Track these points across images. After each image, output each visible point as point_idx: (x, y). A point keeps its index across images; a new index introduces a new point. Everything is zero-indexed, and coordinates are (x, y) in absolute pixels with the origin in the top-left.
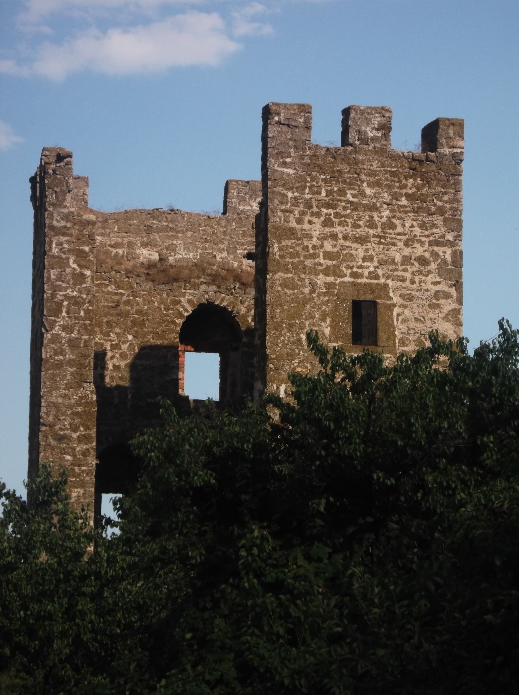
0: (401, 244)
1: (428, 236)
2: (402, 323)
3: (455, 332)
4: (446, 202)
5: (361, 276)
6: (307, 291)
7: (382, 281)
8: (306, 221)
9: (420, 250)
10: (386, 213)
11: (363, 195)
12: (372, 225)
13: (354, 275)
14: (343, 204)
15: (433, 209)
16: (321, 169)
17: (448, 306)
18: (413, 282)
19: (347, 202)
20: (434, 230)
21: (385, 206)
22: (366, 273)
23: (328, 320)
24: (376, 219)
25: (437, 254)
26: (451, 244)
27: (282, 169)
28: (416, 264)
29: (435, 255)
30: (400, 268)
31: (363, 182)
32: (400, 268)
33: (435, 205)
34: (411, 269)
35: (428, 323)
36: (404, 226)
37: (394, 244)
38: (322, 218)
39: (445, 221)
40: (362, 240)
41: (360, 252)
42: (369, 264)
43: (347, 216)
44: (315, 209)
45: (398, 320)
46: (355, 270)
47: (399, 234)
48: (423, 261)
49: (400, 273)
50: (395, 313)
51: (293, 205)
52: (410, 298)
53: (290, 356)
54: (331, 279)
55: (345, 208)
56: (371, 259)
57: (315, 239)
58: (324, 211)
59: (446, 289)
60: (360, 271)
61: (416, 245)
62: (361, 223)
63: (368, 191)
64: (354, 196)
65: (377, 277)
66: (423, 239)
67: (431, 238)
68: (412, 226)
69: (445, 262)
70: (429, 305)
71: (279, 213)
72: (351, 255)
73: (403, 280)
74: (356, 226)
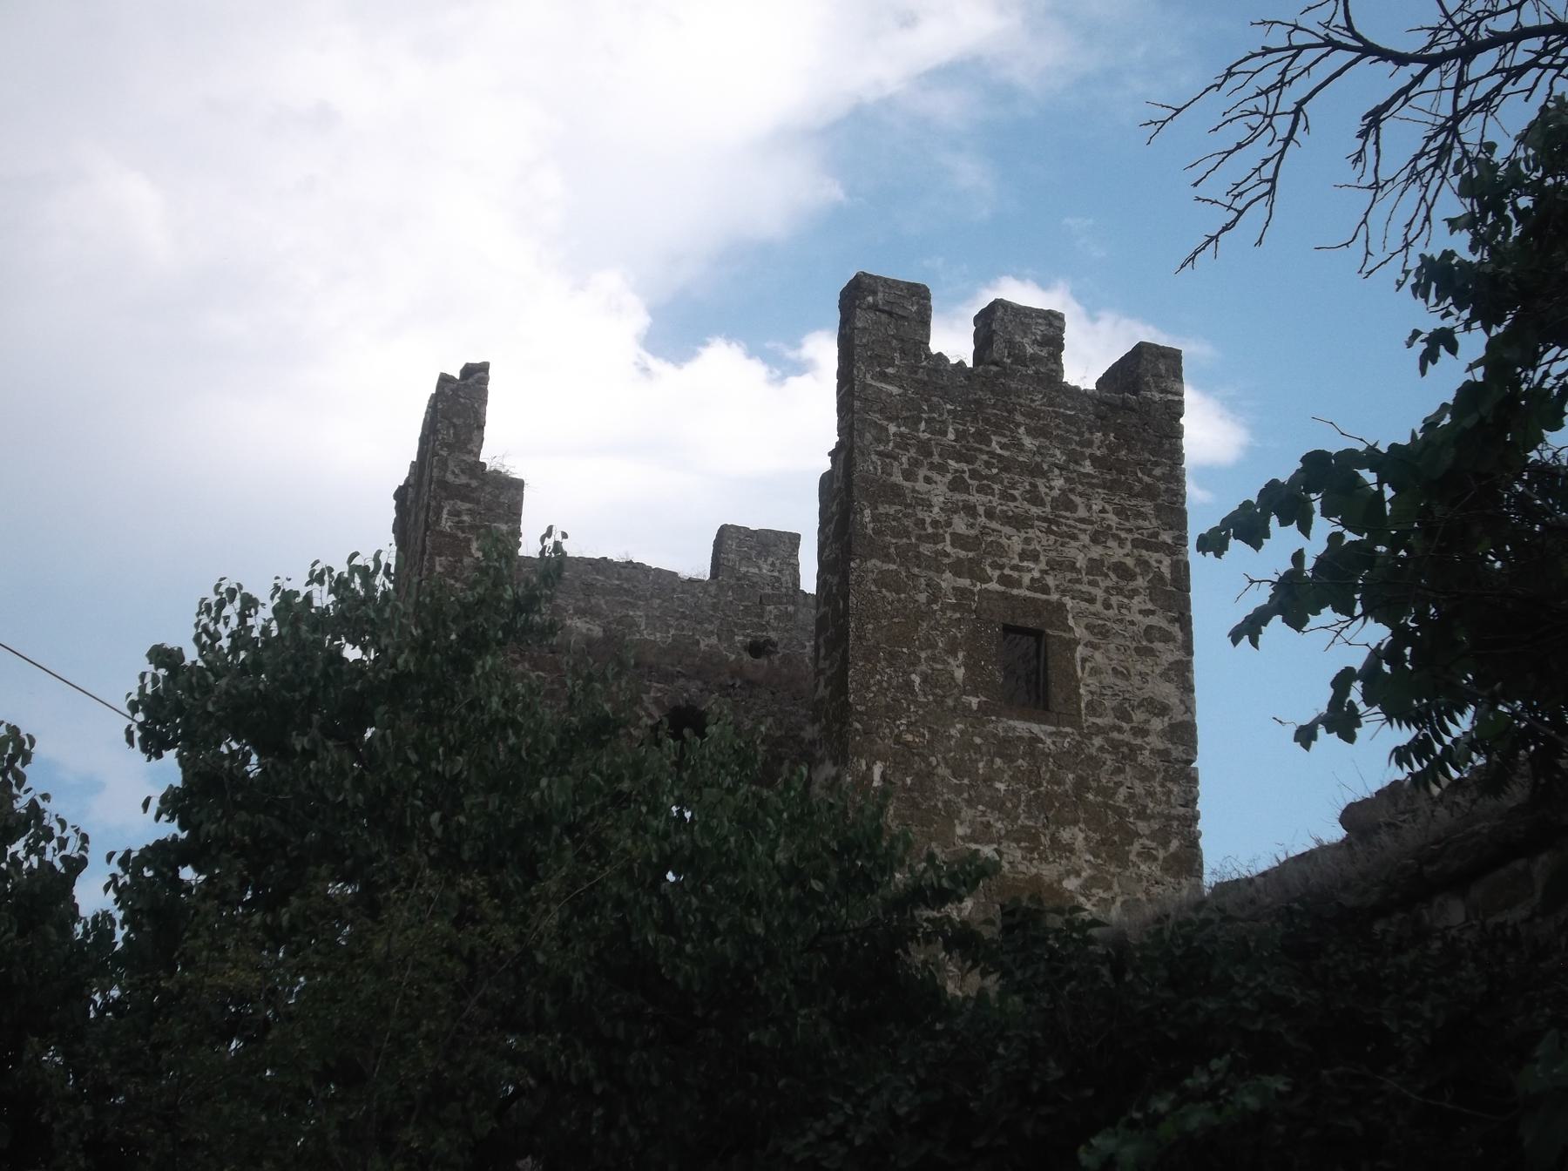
0: (1085, 538)
2: (1090, 675)
3: (1182, 701)
5: (1018, 584)
6: (922, 598)
7: (1055, 597)
8: (921, 477)
9: (1117, 553)
10: (1059, 483)
11: (1020, 447)
12: (1036, 500)
13: (1005, 580)
14: (985, 457)
18: (1108, 606)
19: (992, 454)
20: (1141, 522)
21: (1057, 472)
22: (1026, 579)
23: (961, 655)
24: (1043, 489)
29: (1143, 564)
30: (1085, 579)
31: (1018, 425)
33: (1140, 481)
36: (1089, 508)
37: (1074, 538)
38: (950, 476)
39: (1159, 509)
41: (1015, 542)
44: (936, 459)
45: (1083, 669)
46: (1007, 571)
47: (1082, 520)
48: (1121, 570)
49: (1085, 588)
50: (1078, 655)
51: (897, 446)
52: (1104, 633)
53: (893, 711)
54: (965, 582)
55: (988, 465)
56: (1035, 558)
57: (936, 510)
59: (1164, 624)
60: (1015, 574)
61: (1111, 543)
62: (1016, 493)
63: (1028, 442)
65: (1045, 590)
66: (1123, 535)
68: (1103, 511)
70: (1136, 649)
71: (874, 457)
72: (1000, 545)
73: (1092, 601)
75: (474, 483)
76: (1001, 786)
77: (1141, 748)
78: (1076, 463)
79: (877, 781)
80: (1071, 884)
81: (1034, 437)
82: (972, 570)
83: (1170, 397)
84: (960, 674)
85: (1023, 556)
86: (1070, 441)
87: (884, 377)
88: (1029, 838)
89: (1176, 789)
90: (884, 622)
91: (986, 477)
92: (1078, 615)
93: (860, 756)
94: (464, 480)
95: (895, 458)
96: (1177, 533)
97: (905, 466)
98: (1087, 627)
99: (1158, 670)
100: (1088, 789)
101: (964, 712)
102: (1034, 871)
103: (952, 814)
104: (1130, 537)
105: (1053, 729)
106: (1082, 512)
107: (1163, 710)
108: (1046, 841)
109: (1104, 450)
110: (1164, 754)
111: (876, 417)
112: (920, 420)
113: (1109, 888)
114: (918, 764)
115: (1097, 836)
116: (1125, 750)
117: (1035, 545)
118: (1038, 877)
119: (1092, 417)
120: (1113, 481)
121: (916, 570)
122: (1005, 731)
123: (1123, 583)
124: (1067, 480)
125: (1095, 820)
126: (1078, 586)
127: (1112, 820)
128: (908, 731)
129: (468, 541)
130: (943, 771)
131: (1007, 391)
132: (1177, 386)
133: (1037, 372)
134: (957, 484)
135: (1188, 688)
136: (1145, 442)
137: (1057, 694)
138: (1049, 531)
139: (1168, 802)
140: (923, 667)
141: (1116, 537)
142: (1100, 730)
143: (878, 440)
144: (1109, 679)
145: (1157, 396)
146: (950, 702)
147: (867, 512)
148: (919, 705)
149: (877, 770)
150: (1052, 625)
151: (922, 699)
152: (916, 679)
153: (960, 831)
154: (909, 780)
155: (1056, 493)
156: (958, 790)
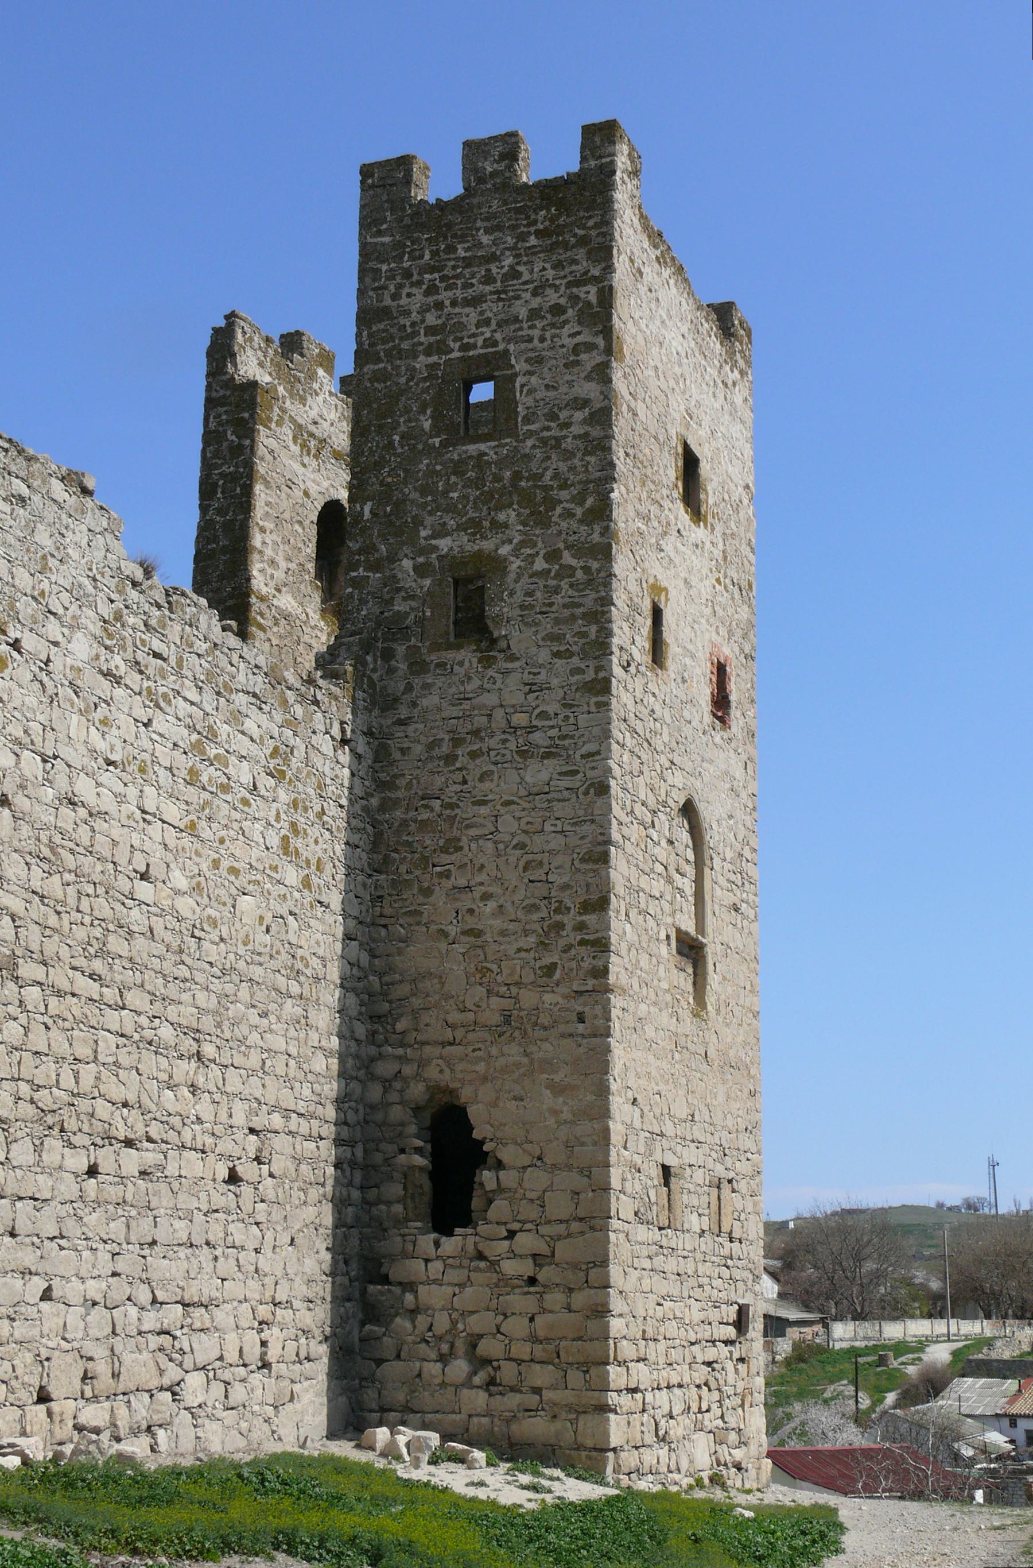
0: (527, 296)
1: (565, 277)
2: (527, 394)
3: (602, 393)
4: (592, 228)
5: (474, 346)
6: (403, 380)
7: (501, 347)
8: (404, 295)
9: (552, 297)
10: (508, 261)
11: (480, 245)
12: (488, 279)
13: (465, 348)
14: (453, 263)
15: (573, 240)
16: (423, 227)
17: (590, 360)
18: (542, 339)
19: (457, 259)
20: (574, 268)
21: (508, 253)
22: (480, 343)
23: (428, 412)
24: (494, 270)
25: (578, 297)
26: (596, 280)
27: (375, 240)
28: (549, 316)
29: (574, 299)
30: (525, 325)
31: (478, 230)
32: (525, 325)
34: (539, 324)
35: (563, 389)
36: (532, 272)
37: (518, 298)
38: (424, 287)
39: (589, 253)
40: (475, 302)
41: (471, 316)
42: (484, 329)
43: (457, 277)
44: (415, 278)
45: (521, 392)
46: (466, 341)
47: (525, 283)
48: (557, 310)
50: (518, 385)
51: (388, 278)
54: (434, 359)
55: (454, 268)
56: (487, 322)
57: (414, 314)
58: (427, 276)
60: (472, 341)
61: (549, 291)
62: (474, 281)
63: (485, 239)
64: (466, 250)
65: (495, 344)
66: (557, 282)
67: (570, 278)
68: (544, 269)
69: (589, 304)
70: (566, 365)
71: (371, 293)
73: (530, 340)
74: (467, 286)
75: (228, 393)
77: (565, 437)
78: (524, 241)
79: (367, 514)
80: (504, 550)
82: (441, 348)
84: (427, 425)
86: (518, 226)
87: (380, 233)
88: (474, 528)
90: (375, 406)
94: (222, 393)
96: (603, 265)
98: (526, 361)
99: (583, 375)
100: (521, 480)
101: (430, 449)
102: (476, 548)
103: (418, 522)
106: (526, 277)
107: (586, 402)
108: (486, 524)
109: (547, 223)
112: (404, 253)
113: (535, 545)
114: (397, 495)
115: (528, 511)
116: (553, 442)
119: (538, 202)
120: (552, 245)
124: (516, 256)
125: (527, 499)
126: (520, 333)
127: (539, 495)
128: (389, 475)
129: (225, 432)
130: (415, 495)
131: (471, 207)
132: (610, 149)
136: (580, 203)
138: (503, 300)
139: (587, 471)
140: (403, 428)
141: (550, 286)
142: (531, 434)
143: (374, 280)
144: (539, 395)
146: (420, 447)
148: (399, 455)
150: (499, 369)
151: (399, 450)
152: (396, 438)
153: (423, 533)
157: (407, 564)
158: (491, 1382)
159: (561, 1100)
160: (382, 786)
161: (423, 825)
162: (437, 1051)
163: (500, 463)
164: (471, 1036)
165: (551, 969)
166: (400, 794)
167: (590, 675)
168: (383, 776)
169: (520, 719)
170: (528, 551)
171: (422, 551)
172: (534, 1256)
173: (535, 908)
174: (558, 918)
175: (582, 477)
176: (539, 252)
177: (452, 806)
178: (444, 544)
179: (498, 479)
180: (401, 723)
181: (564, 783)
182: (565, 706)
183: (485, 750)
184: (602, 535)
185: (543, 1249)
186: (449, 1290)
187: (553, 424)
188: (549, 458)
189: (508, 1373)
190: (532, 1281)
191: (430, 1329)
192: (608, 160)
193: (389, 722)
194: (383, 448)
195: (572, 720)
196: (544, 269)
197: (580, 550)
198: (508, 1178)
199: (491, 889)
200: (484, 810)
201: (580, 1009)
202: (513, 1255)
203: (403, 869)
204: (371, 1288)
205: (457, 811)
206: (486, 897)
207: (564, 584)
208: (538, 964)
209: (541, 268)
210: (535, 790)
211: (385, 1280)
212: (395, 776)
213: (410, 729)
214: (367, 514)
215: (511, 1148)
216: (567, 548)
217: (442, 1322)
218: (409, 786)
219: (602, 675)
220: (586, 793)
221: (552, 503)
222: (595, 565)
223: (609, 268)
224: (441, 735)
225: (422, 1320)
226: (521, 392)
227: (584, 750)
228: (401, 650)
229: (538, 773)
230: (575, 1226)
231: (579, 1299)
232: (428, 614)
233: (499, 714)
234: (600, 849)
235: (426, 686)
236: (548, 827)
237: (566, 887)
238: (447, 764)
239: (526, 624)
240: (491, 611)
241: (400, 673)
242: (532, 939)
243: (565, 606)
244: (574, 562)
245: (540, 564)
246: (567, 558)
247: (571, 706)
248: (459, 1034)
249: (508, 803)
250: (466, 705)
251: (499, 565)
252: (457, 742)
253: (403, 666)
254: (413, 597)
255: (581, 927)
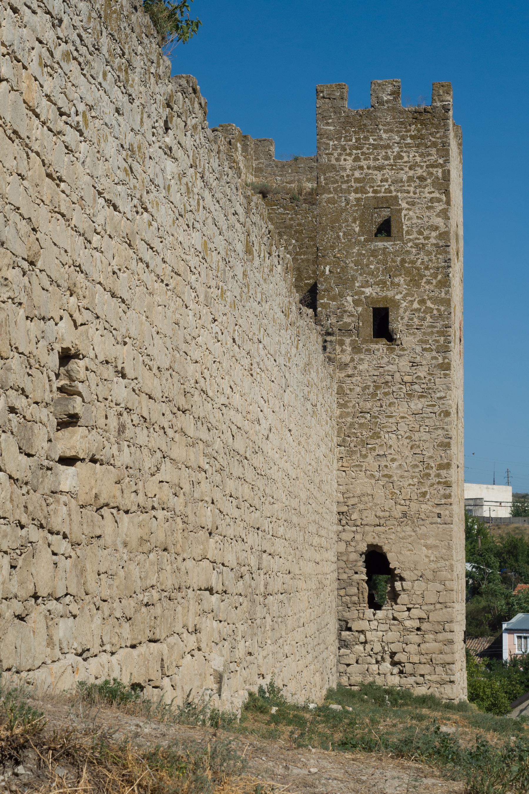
0: (407, 169)
1: (425, 162)
2: (407, 220)
3: (445, 224)
4: (438, 138)
5: (380, 192)
6: (343, 204)
7: (394, 194)
8: (342, 159)
9: (419, 172)
10: (396, 149)
11: (381, 139)
12: (387, 158)
13: (375, 192)
14: (367, 146)
15: (429, 144)
17: (439, 207)
18: (415, 193)
19: (370, 144)
20: (429, 158)
21: (396, 145)
22: (383, 190)
23: (357, 223)
24: (390, 153)
25: (432, 173)
27: (326, 127)
28: (417, 180)
30: (406, 185)
31: (380, 130)
32: (406, 185)
33: (430, 141)
35: (426, 219)
36: (409, 156)
37: (402, 169)
38: (353, 157)
39: (438, 150)
40: (380, 168)
41: (378, 176)
42: (385, 184)
43: (370, 154)
44: (348, 151)
45: (405, 219)
46: (375, 188)
47: (406, 162)
48: (422, 179)
49: (406, 188)
50: (403, 214)
51: (333, 149)
53: (333, 247)
54: (359, 195)
56: (387, 181)
57: (348, 170)
59: (438, 195)
60: (379, 188)
62: (379, 157)
63: (384, 136)
64: (374, 140)
65: (390, 192)
66: (422, 164)
67: (428, 163)
68: (415, 156)
69: (437, 178)
70: (426, 208)
71: (324, 156)
72: (373, 178)
73: (409, 192)
76: (372, 267)
77: (427, 244)
78: (404, 140)
79: (327, 272)
80: (398, 297)
81: (387, 133)
82: (362, 190)
83: (444, 103)
84: (357, 229)
85: (382, 181)
87: (328, 124)
89: (441, 257)
91: (367, 154)
92: (405, 198)
93: (321, 265)
95: (332, 154)
97: (336, 156)
98: (407, 203)
100: (406, 262)
104: (425, 164)
105: (392, 243)
107: (437, 228)
109: (416, 132)
110: (437, 245)
111: (324, 140)
114: (342, 264)
115: (409, 279)
116: (421, 246)
117: (387, 176)
118: (386, 297)
120: (419, 144)
121: (340, 195)
122: (374, 247)
123: (421, 183)
124: (400, 147)
125: (408, 273)
130: (352, 265)
131: (376, 118)
133: (388, 107)
134: (357, 159)
135: (447, 218)
137: (394, 230)
138: (394, 169)
139: (438, 262)
140: (344, 229)
141: (418, 166)
142: (410, 240)
143: (326, 149)
144: (414, 221)
145: (439, 104)
146: (354, 240)
147: (322, 177)
149: (327, 269)
150: (393, 205)
151: (343, 241)
152: (341, 234)
153: (357, 285)
154: (339, 270)
155: (395, 154)
156: (357, 270)
157: (349, 299)
158: (401, 672)
159: (430, 551)
160: (340, 406)
161: (361, 425)
162: (372, 528)
163: (396, 253)
164: (388, 522)
165: (424, 494)
166: (349, 410)
167: (440, 361)
168: (341, 401)
169: (407, 378)
170: (410, 299)
171: (357, 293)
172: (419, 619)
173: (416, 466)
174: (428, 471)
175: (435, 265)
176: (413, 147)
177: (376, 417)
178: (368, 291)
179: (394, 261)
180: (349, 376)
181: (430, 410)
182: (429, 374)
183: (391, 392)
184: (446, 294)
185: (425, 616)
186: (381, 633)
187: (421, 237)
188: (418, 254)
189: (408, 668)
190: (418, 629)
191: (372, 650)
192: (447, 103)
193: (343, 375)
194: (334, 239)
195: (433, 381)
196: (415, 156)
197: (436, 301)
198: (407, 585)
199: (395, 457)
200: (390, 420)
201: (438, 512)
202: (410, 618)
203: (352, 445)
204: (343, 633)
205: (378, 420)
206: (393, 460)
207: (428, 317)
208: (419, 491)
209: (412, 156)
210: (415, 412)
211: (349, 629)
212: (347, 401)
213: (354, 379)
214: (327, 272)
215: (408, 572)
216: (430, 299)
217: (377, 648)
218: (354, 406)
219: (447, 361)
220: (440, 415)
221: (422, 276)
222: (443, 308)
223: (447, 161)
224: (369, 383)
225: (368, 647)
226: (405, 219)
227: (438, 395)
228: (348, 341)
229: (417, 405)
230: (438, 606)
231: (440, 637)
232: (361, 324)
233: (397, 376)
234: (448, 440)
235: (362, 360)
236: (422, 429)
237: (431, 457)
238: (372, 398)
239: (410, 334)
240: (392, 326)
241: (348, 352)
242: (416, 480)
243: (429, 327)
244: (432, 306)
245: (416, 305)
246: (429, 304)
247: (432, 374)
248: (382, 521)
249: (403, 418)
250: (381, 370)
251: (397, 304)
252: (377, 387)
253: (349, 349)
254: (353, 316)
255: (438, 476)
